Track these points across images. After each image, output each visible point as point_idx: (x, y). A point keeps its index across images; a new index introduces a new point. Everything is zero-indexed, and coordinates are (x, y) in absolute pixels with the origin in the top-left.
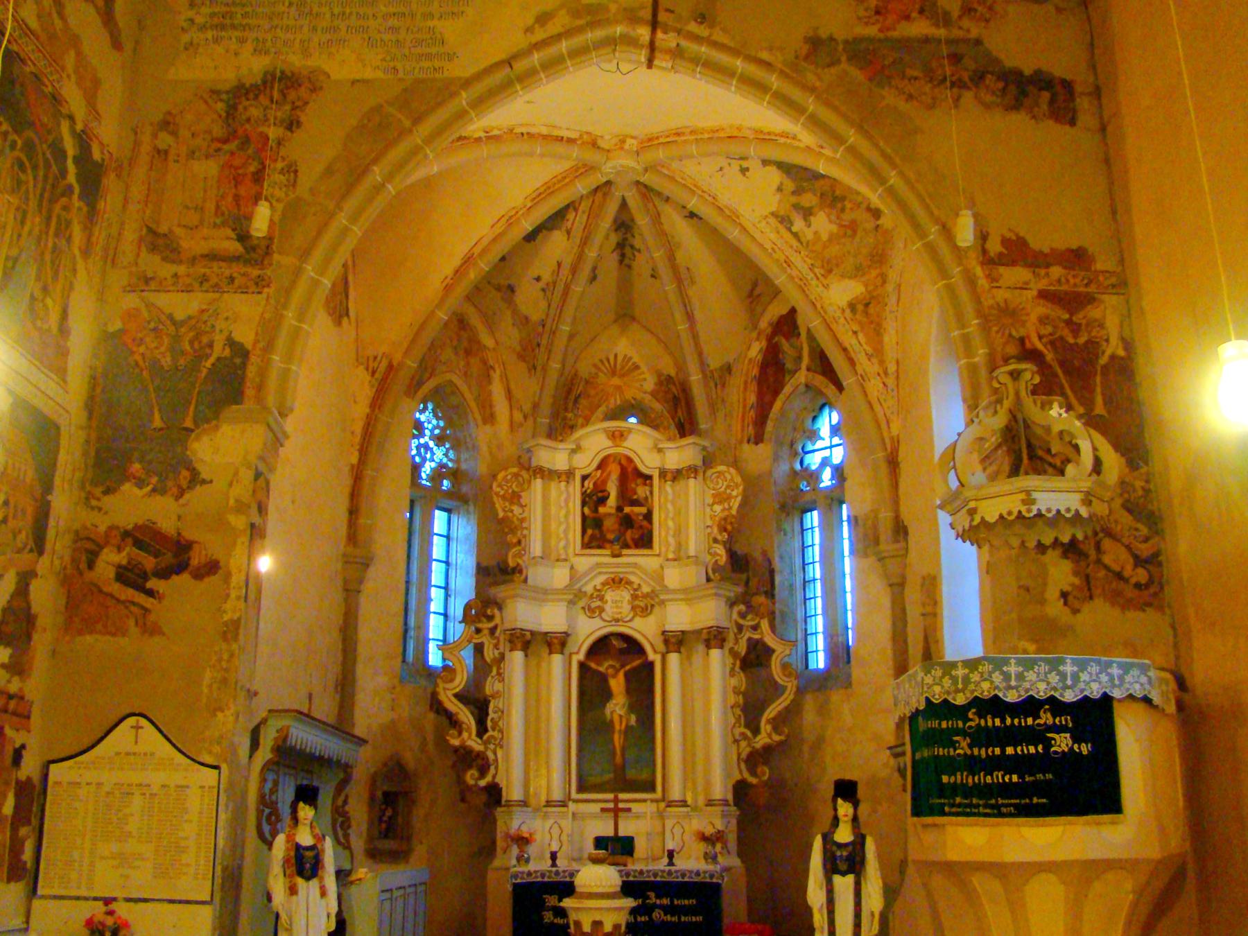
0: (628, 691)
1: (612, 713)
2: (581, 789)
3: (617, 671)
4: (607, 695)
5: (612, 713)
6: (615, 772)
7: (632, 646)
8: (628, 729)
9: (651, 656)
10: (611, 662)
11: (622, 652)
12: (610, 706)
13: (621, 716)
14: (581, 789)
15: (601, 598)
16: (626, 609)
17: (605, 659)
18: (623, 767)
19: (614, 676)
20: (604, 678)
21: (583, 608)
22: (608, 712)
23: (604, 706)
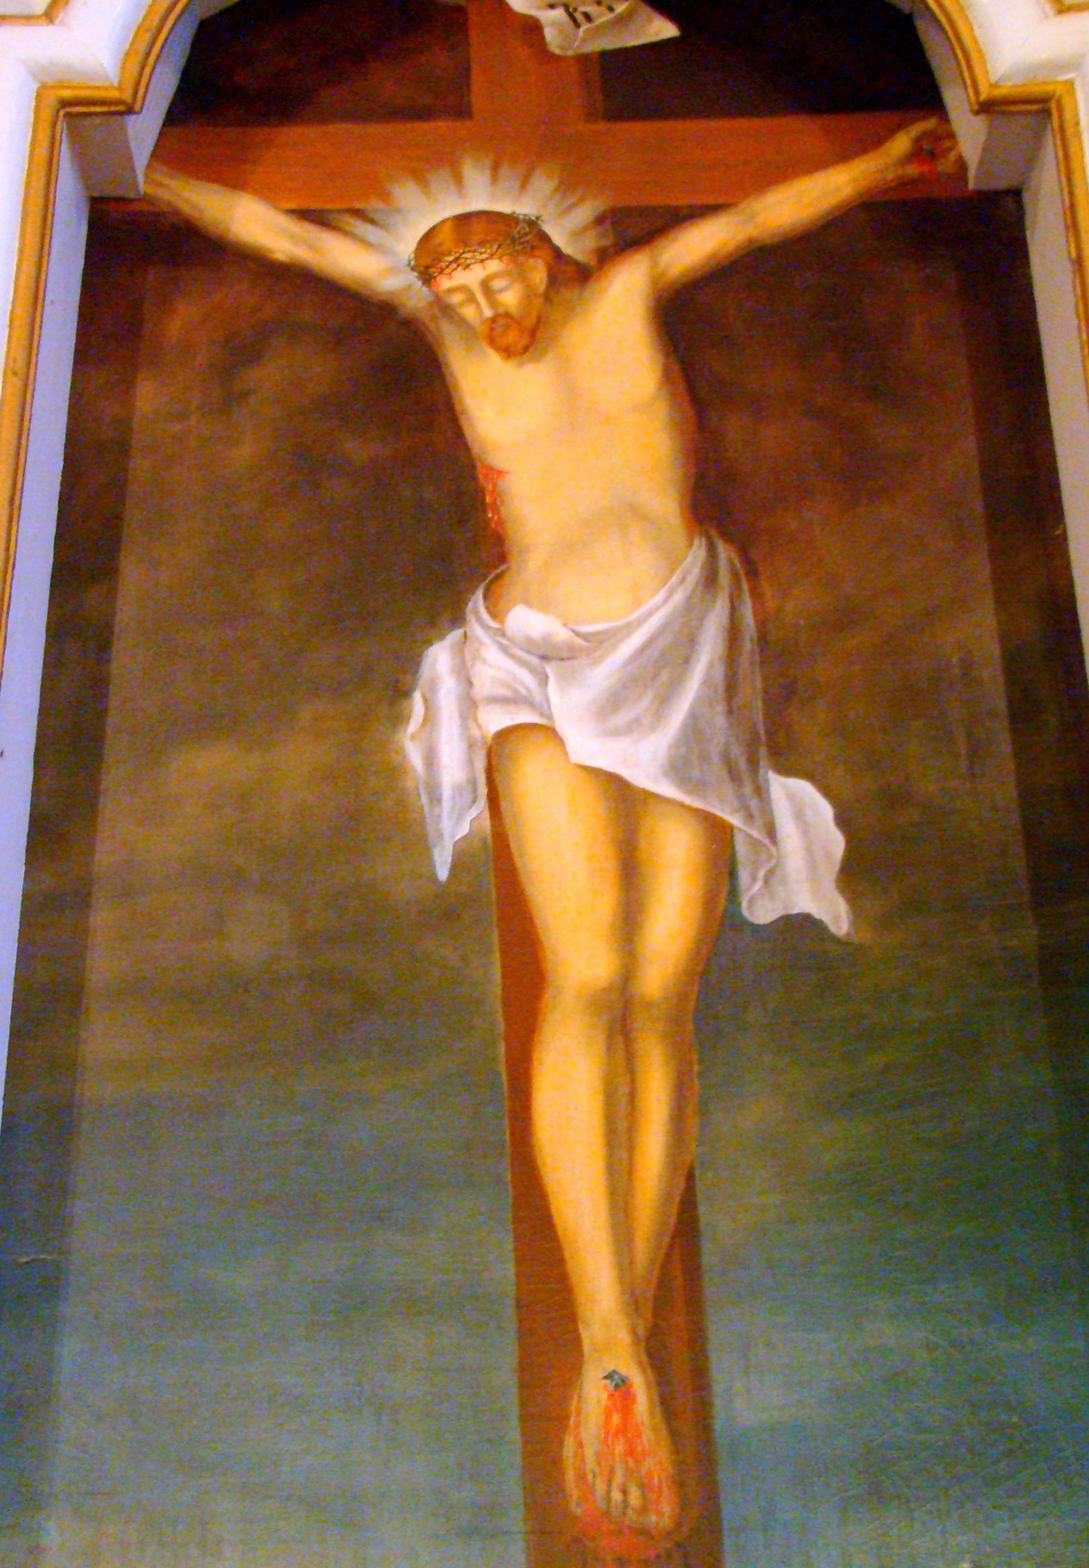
0: (718, 500)
3: (572, 276)
4: (438, 538)
5: (497, 758)
8: (745, 986)
10: (480, 193)
12: (463, 688)
13: (624, 801)
17: (444, 161)
19: (524, 337)
20: (392, 370)
22: (438, 741)
23: (396, 686)
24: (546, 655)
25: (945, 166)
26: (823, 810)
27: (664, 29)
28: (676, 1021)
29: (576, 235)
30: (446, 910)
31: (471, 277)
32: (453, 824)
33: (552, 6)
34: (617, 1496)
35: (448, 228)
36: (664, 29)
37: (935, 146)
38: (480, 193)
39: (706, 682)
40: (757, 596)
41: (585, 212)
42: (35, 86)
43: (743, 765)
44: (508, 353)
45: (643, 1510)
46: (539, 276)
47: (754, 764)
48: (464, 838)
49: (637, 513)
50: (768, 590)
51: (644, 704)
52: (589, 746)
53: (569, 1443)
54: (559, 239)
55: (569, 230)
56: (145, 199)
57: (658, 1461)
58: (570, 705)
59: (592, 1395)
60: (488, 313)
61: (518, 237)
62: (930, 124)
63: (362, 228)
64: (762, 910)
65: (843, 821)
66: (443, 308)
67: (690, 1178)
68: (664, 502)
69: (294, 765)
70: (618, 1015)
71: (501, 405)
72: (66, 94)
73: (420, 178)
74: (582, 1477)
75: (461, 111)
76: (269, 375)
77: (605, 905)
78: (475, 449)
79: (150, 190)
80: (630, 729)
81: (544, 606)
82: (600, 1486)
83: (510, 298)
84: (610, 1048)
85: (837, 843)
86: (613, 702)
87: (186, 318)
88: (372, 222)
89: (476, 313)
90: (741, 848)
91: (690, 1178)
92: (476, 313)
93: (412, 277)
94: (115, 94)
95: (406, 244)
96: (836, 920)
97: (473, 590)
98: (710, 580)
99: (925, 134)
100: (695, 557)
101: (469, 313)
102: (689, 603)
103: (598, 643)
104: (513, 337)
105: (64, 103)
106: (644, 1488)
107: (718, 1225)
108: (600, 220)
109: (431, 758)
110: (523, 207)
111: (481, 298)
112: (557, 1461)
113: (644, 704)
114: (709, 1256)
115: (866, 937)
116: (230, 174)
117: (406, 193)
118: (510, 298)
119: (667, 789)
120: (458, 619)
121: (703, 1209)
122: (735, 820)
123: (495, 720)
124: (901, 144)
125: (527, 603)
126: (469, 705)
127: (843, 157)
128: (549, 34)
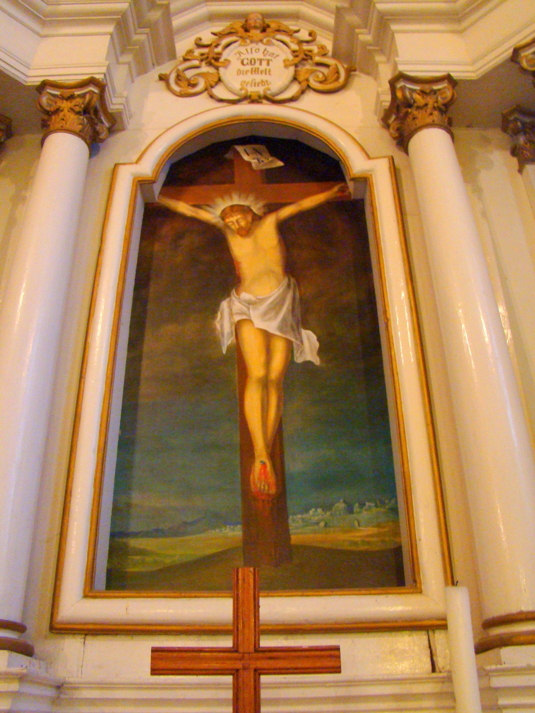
0: (291, 268)
1: (237, 327)
2: (117, 575)
3: (257, 219)
4: (224, 277)
5: (237, 327)
6: (248, 521)
7: (306, 159)
8: (295, 375)
9: (356, 163)
10: (236, 200)
11: (270, 176)
13: (267, 336)
14: (117, 575)
15: (213, 61)
16: (279, 77)
17: (227, 193)
18: (279, 505)
20: (215, 240)
21: (163, 78)
23: (214, 310)
24: (250, 303)
25: (346, 194)
26: (314, 337)
27: (280, 164)
28: (278, 384)
29: (259, 209)
30: (224, 360)
31: (234, 219)
32: (227, 341)
33: (254, 159)
34: (262, 487)
35: (228, 209)
36: (280, 164)
37: (344, 190)
38: (236, 200)
39: (288, 309)
40: (300, 290)
41: (261, 204)
42: (132, 178)
43: (295, 327)
44: (242, 236)
45: (268, 490)
46: (250, 218)
47: (298, 328)
48: (230, 344)
49: (272, 272)
50: (302, 289)
51: (272, 314)
52: (259, 323)
53: (252, 477)
54: (255, 210)
55: (257, 208)
56: (157, 203)
57: (272, 479)
58: (255, 315)
59: (257, 467)
60: (237, 227)
61: (244, 210)
62: (342, 184)
63: (209, 209)
64: (299, 359)
65: (319, 340)
66: (227, 226)
67: (281, 418)
68: (278, 269)
69: (190, 328)
70: (265, 383)
71: (240, 248)
72: (140, 179)
73: (222, 197)
74: (254, 479)
75: (233, 183)
76: (185, 242)
77: (263, 359)
78: (234, 258)
79: (159, 201)
80: (269, 319)
81: (250, 292)
82: (259, 486)
83: (243, 223)
84: (263, 390)
85: (317, 345)
86: (265, 314)
87: (167, 230)
88: (211, 207)
89: (235, 227)
90: (295, 345)
91: (281, 418)
92: (235, 227)
93: (220, 219)
94: (151, 179)
95: (218, 212)
96: (317, 362)
97: (232, 289)
98: (289, 286)
99: (342, 187)
100: (286, 280)
101: (233, 227)
102: (283, 291)
103: (262, 301)
104: (243, 232)
105: (139, 181)
106: (269, 485)
107: (288, 431)
108: (264, 206)
109: (222, 326)
110: (246, 203)
111: (236, 224)
112: (249, 481)
113: (272, 314)
114: (285, 435)
115: (324, 365)
116: (177, 197)
117: (219, 201)
118: (243, 223)
119: (277, 333)
120: (229, 295)
121: (284, 426)
122: (293, 339)
123: (237, 318)
124: (336, 189)
125: (245, 291)
126: (231, 314)
127: (322, 191)
128: (253, 165)
